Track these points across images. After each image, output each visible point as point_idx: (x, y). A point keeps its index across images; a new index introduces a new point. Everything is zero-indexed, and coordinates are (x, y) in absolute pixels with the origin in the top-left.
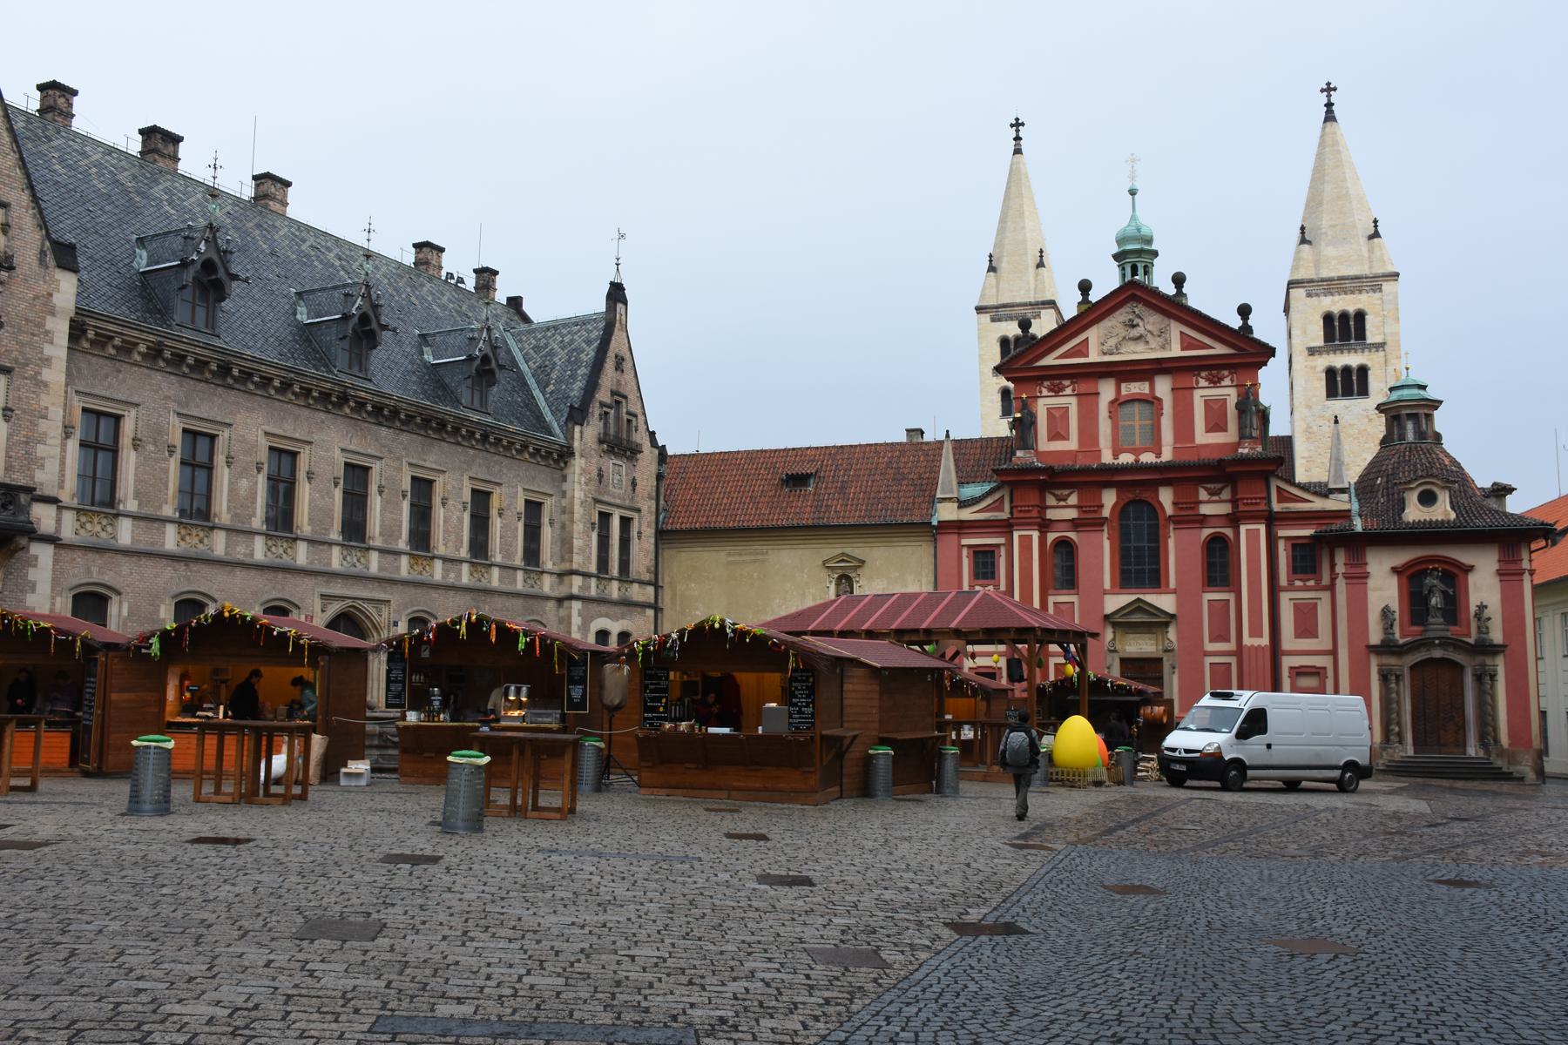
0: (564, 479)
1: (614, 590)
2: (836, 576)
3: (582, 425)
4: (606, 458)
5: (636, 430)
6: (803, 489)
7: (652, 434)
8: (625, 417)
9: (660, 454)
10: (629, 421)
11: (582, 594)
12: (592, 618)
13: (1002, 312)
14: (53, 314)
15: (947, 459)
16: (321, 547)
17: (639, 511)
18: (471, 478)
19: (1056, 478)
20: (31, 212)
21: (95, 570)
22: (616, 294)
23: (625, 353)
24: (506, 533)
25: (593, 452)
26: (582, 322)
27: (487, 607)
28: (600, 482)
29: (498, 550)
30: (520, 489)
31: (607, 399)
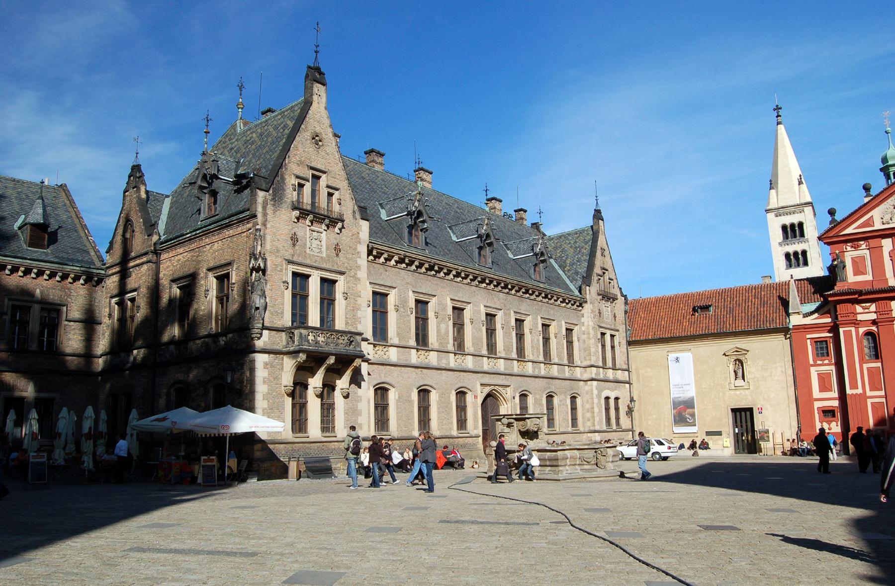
1: (610, 374)
2: (733, 360)
6: (707, 313)
7: (620, 289)
9: (625, 299)
10: (610, 283)
13: (781, 211)
14: (360, 243)
15: (793, 291)
19: (859, 296)
20: (349, 192)
21: (383, 375)
22: (598, 215)
24: (557, 345)
26: (579, 233)
30: (563, 323)
31: (600, 272)
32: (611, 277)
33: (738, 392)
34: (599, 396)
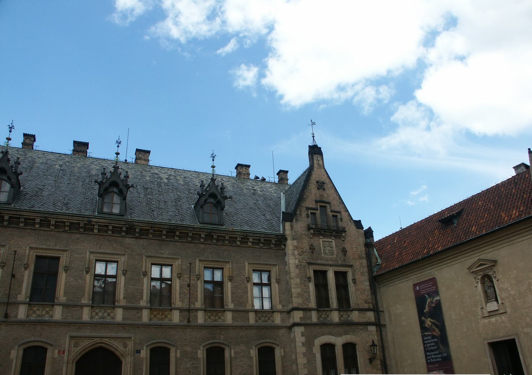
0: (285, 254)
2: (480, 277)
3: (291, 221)
4: (316, 238)
5: (341, 221)
8: (331, 214)
11: (301, 322)
12: (316, 337)
16: (74, 309)
17: (351, 266)
18: (200, 261)
23: (324, 179)
25: (303, 236)
27: (222, 337)
28: (313, 252)
29: (230, 301)
30: (246, 264)
31: (312, 205)
32: (337, 209)
33: (493, 319)
34: (309, 344)
